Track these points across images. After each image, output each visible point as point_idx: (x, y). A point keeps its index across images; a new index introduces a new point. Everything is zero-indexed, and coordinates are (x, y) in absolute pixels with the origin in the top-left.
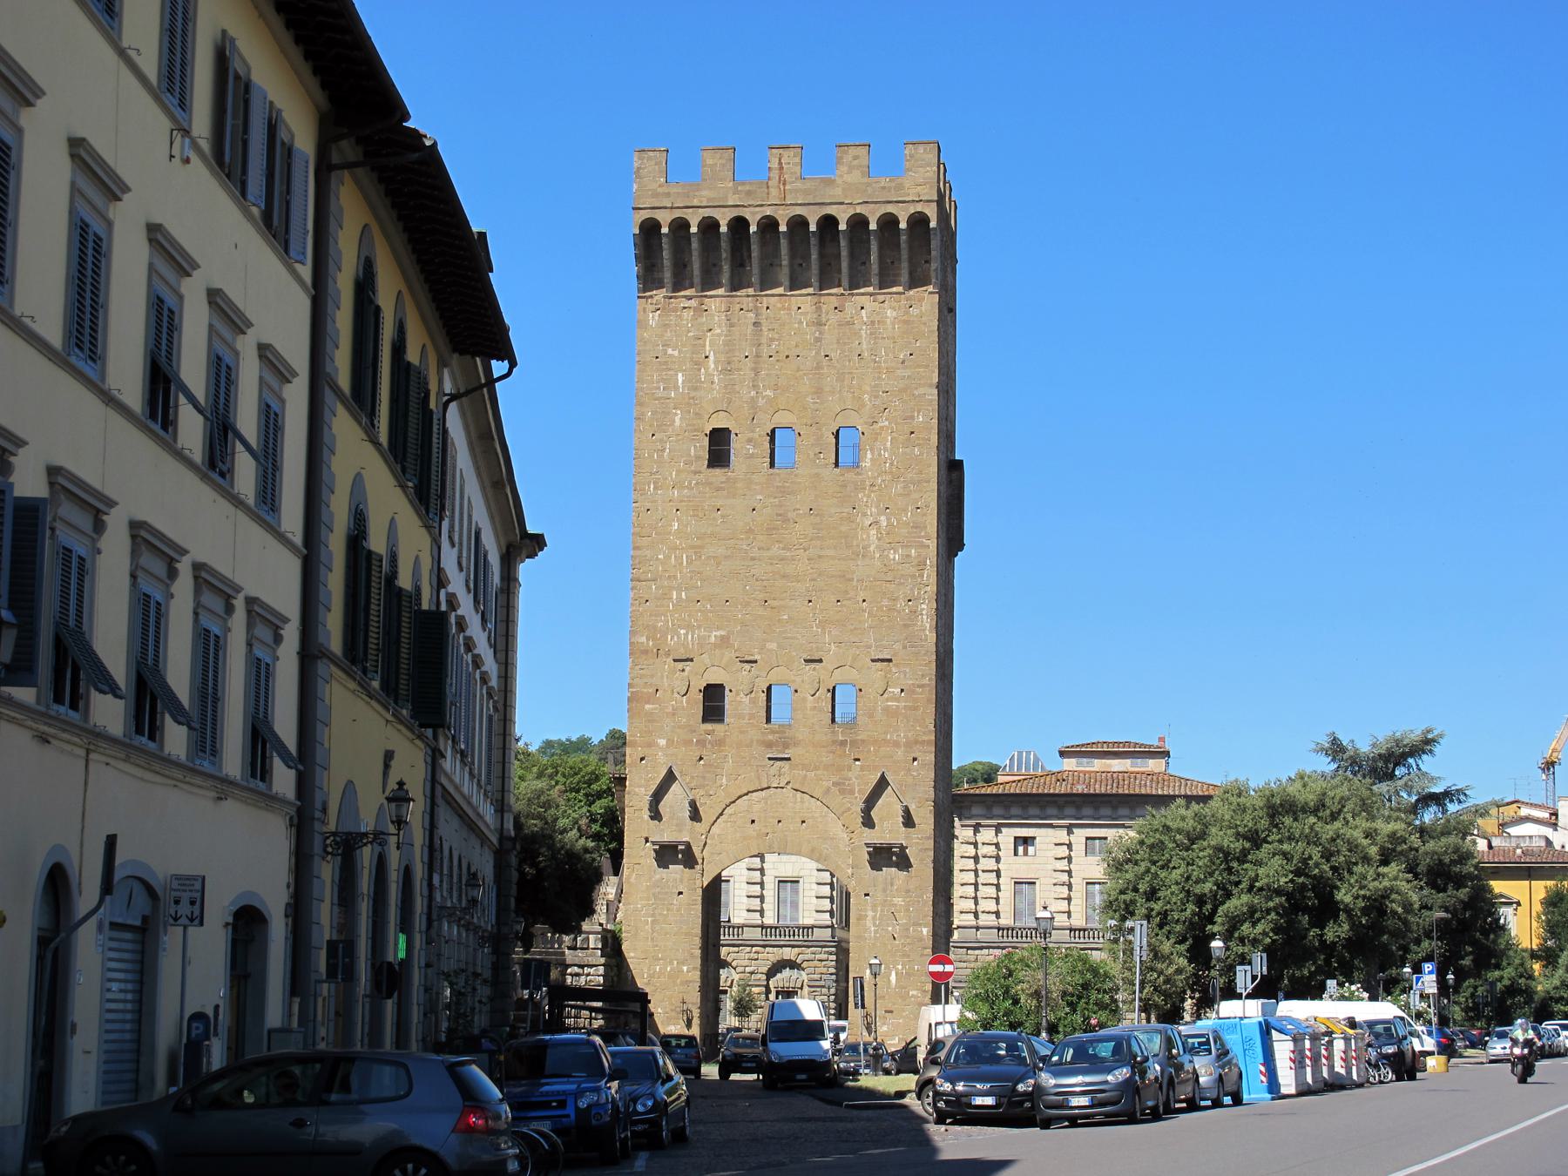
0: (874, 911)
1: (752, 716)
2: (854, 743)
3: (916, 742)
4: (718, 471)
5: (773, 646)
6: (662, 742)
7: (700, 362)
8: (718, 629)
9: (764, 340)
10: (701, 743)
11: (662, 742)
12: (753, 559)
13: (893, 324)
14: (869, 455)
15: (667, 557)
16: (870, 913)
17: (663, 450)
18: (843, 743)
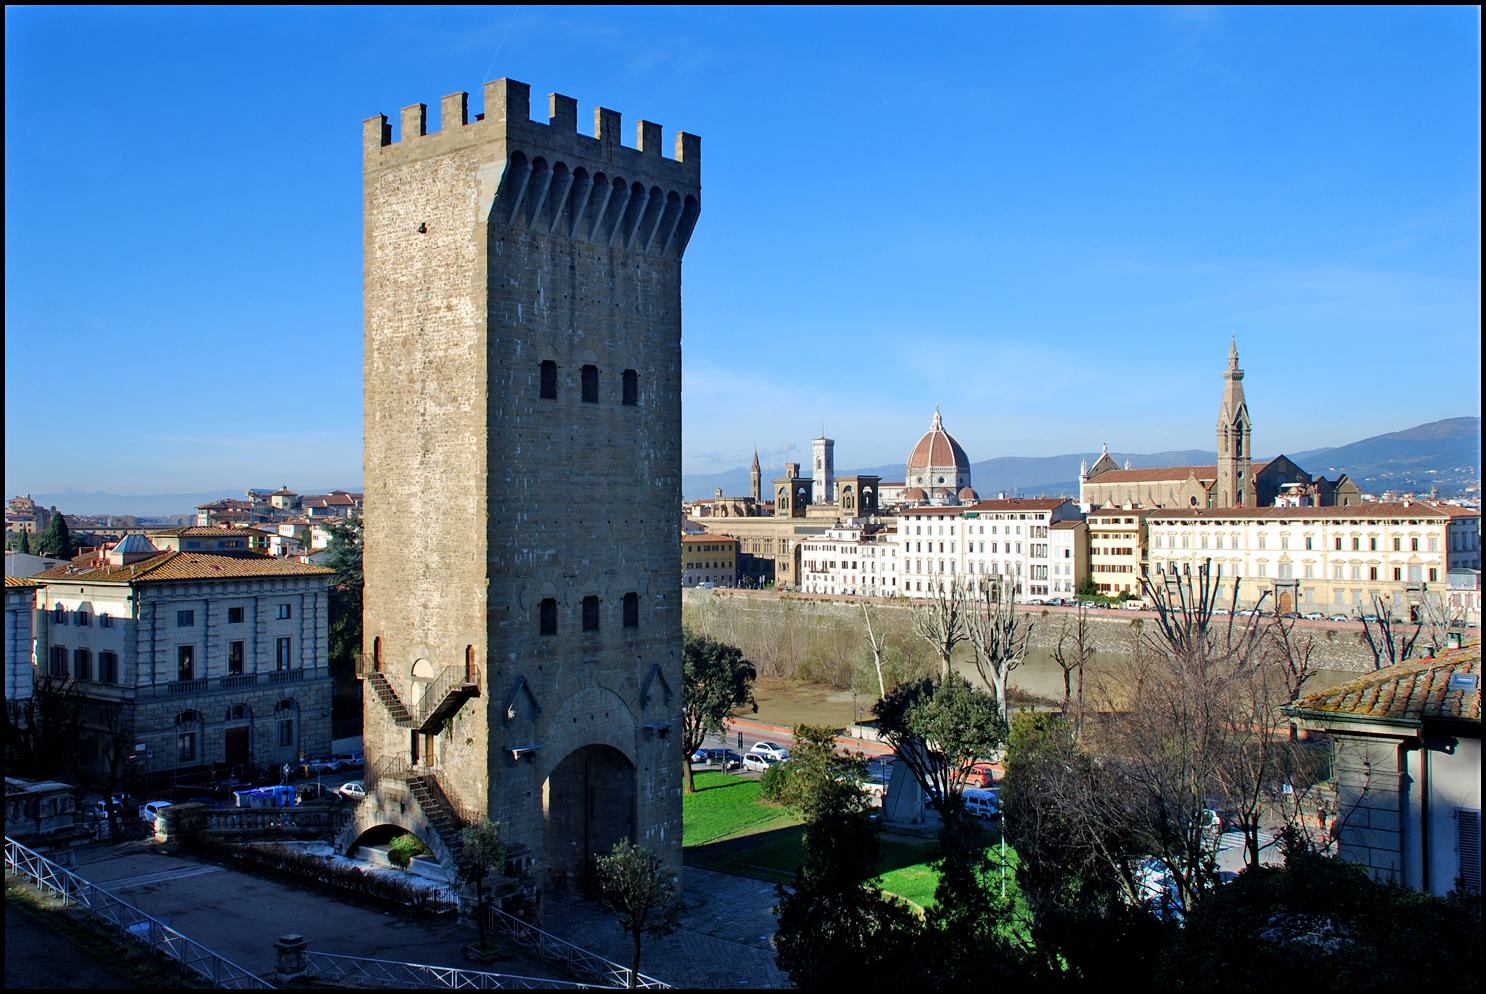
0: (651, 781)
1: (574, 626)
2: (638, 643)
3: (672, 639)
4: (547, 402)
5: (586, 562)
6: (513, 656)
7: (533, 297)
8: (550, 547)
9: (577, 283)
10: (541, 654)
11: (513, 656)
12: (572, 484)
13: (656, 284)
14: (643, 397)
15: (513, 481)
16: (649, 784)
17: (509, 378)
18: (630, 644)
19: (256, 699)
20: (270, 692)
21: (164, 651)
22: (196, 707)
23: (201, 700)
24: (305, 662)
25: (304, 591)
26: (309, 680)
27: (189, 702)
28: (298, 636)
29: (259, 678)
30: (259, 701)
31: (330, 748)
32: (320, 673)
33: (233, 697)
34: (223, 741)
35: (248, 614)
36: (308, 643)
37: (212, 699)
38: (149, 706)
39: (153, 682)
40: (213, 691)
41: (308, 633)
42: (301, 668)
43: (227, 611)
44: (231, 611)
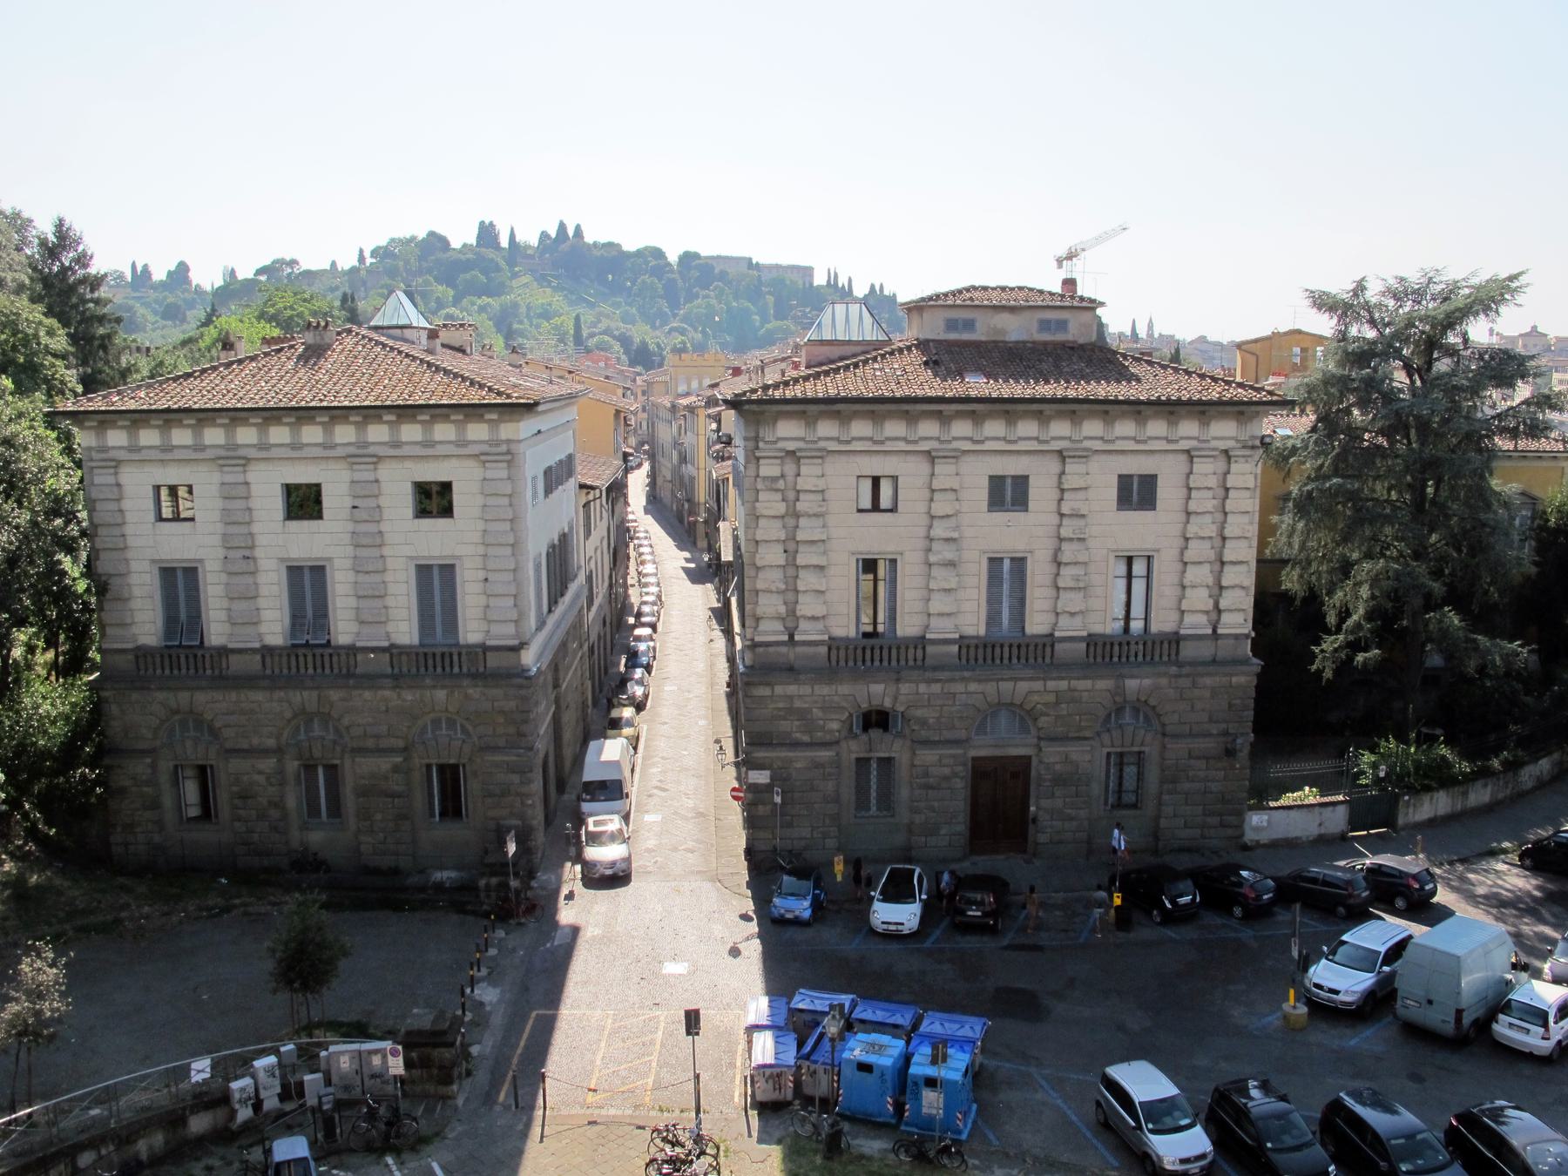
19: (1051, 698)
20: (1087, 684)
21: (821, 568)
22: (896, 698)
23: (905, 688)
24: (1188, 619)
25: (1194, 443)
26: (1194, 663)
27: (877, 688)
28: (1175, 552)
29: (1057, 647)
30: (1057, 703)
31: (1240, 826)
32: (1224, 650)
33: (990, 688)
34: (960, 785)
35: (1041, 492)
36: (1200, 575)
37: (936, 688)
38: (779, 690)
39: (791, 636)
40: (935, 669)
41: (1197, 550)
42: (1177, 633)
43: (985, 482)
44: (996, 482)
